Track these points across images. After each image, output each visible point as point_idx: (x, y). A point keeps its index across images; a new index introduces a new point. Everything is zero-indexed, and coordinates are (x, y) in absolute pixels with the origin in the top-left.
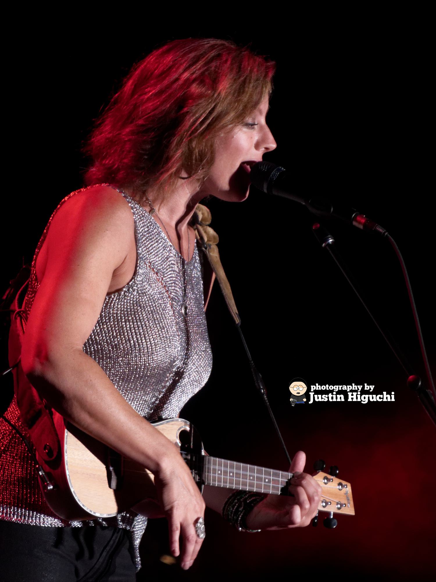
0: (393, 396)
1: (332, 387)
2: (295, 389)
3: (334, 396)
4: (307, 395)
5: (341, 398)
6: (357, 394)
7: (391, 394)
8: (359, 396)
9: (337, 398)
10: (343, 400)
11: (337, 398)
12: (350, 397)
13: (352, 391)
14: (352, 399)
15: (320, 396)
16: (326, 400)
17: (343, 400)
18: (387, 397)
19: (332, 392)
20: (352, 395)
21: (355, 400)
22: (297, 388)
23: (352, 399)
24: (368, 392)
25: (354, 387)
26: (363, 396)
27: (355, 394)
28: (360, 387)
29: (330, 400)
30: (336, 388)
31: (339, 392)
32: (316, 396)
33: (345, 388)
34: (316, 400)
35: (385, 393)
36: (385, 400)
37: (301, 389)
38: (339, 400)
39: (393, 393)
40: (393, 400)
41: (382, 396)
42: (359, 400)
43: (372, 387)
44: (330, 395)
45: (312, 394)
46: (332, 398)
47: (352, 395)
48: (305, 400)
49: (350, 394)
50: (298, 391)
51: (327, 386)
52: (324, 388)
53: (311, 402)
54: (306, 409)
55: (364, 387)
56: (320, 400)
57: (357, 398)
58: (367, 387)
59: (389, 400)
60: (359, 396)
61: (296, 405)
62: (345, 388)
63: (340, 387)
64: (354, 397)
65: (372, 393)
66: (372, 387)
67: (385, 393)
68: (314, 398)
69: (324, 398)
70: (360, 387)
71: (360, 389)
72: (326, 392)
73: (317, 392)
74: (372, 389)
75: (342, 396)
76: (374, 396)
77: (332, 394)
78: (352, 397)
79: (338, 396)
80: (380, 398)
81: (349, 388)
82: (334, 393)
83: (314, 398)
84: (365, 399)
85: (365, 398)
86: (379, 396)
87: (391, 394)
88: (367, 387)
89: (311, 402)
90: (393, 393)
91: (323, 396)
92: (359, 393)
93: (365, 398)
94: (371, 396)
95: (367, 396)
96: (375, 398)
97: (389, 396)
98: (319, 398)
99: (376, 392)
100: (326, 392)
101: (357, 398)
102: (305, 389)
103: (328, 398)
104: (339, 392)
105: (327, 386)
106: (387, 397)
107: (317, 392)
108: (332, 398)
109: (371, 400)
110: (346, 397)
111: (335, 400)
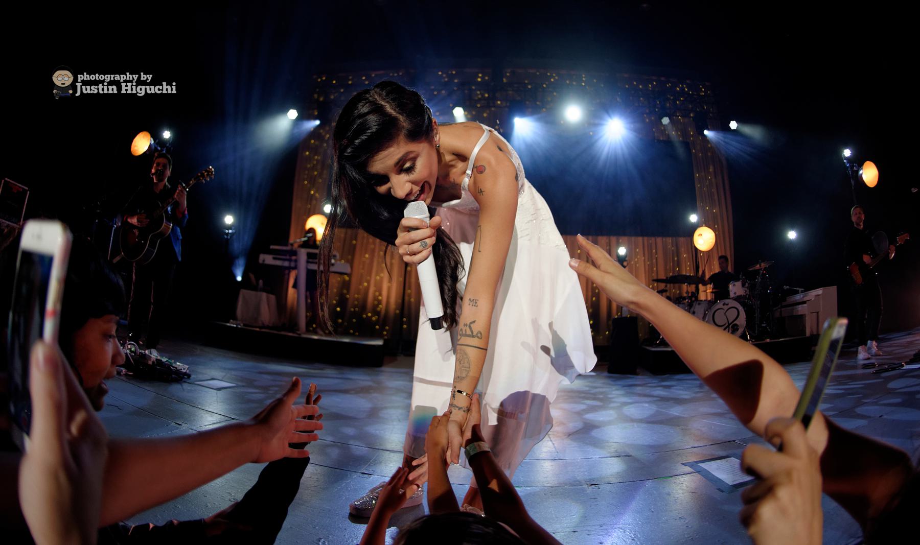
0: (174, 88)
1: (102, 77)
3: (105, 88)
4: (73, 86)
5: (113, 89)
6: (132, 85)
7: (171, 85)
8: (134, 87)
10: (115, 92)
12: (124, 88)
13: (126, 81)
15: (88, 87)
16: (96, 91)
17: (115, 92)
18: (168, 89)
19: (102, 82)
21: (129, 91)
22: (62, 78)
24: (144, 83)
25: (129, 76)
26: (139, 87)
27: (129, 84)
28: (136, 77)
29: (101, 92)
30: (108, 78)
31: (111, 83)
32: (84, 87)
33: (117, 77)
34: (84, 92)
35: (164, 84)
36: (165, 92)
38: (110, 92)
40: (174, 91)
42: (134, 92)
43: (150, 77)
44: (100, 86)
45: (79, 85)
46: (103, 89)
48: (71, 92)
49: (123, 85)
53: (78, 94)
54: (71, 102)
55: (140, 77)
56: (89, 91)
58: (143, 77)
59: (169, 92)
60: (134, 87)
61: (61, 98)
62: (117, 77)
64: (129, 88)
65: (150, 84)
66: (150, 77)
67: (164, 84)
69: (93, 90)
70: (136, 77)
72: (96, 83)
73: (85, 83)
75: (115, 87)
76: (152, 87)
77: (103, 85)
78: (126, 89)
79: (110, 87)
81: (122, 78)
84: (141, 91)
86: (157, 87)
87: (171, 85)
88: (143, 77)
89: (78, 94)
91: (93, 87)
94: (148, 87)
95: (143, 87)
96: (153, 90)
97: (169, 87)
98: (87, 90)
99: (154, 83)
100: (96, 83)
104: (111, 83)
106: (168, 89)
107: (85, 83)
108: (103, 89)
109: (149, 92)
111: (106, 92)
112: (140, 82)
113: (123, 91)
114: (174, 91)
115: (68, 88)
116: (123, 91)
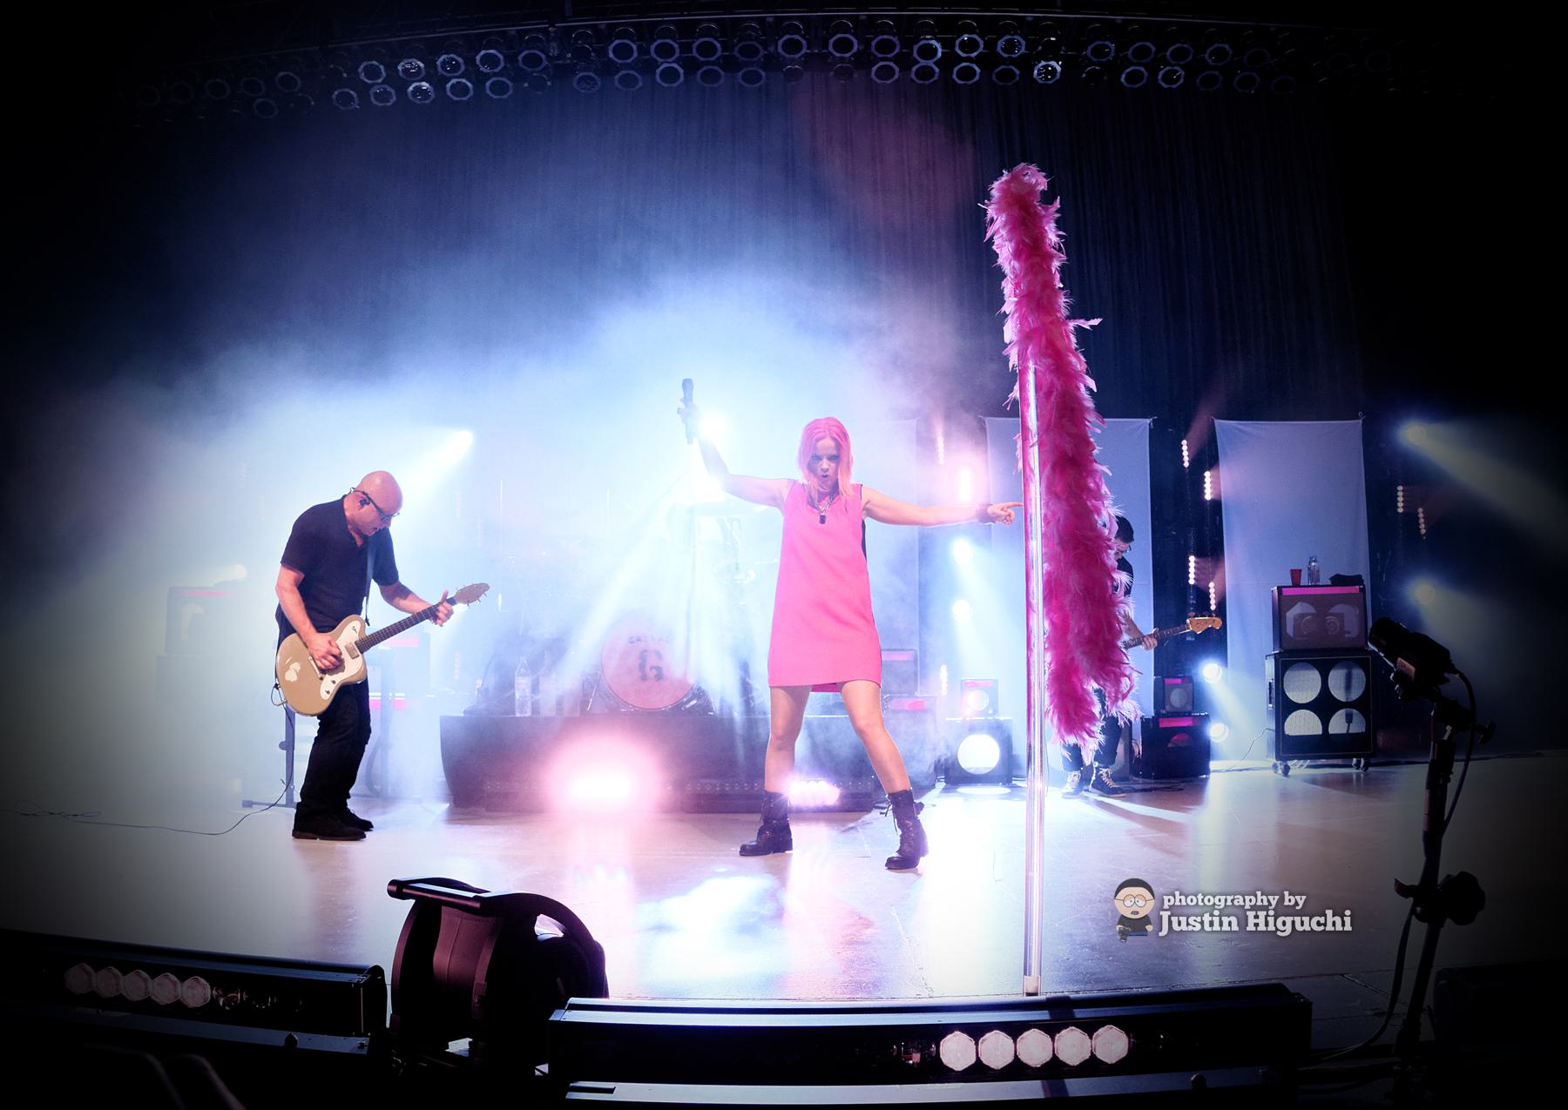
0: (1348, 920)
2: (1128, 903)
3: (1216, 920)
8: (1271, 920)
9: (1221, 924)
11: (1221, 924)
12: (1251, 921)
13: (1253, 908)
14: (1256, 925)
15: (1183, 919)
17: (1235, 927)
20: (1256, 917)
21: (1262, 928)
23: (1256, 925)
24: (1292, 911)
26: (1280, 920)
27: (1262, 914)
28: (1274, 900)
29: (1207, 928)
34: (1175, 927)
35: (1329, 913)
36: (1330, 928)
37: (1141, 903)
38: (1226, 927)
39: (1348, 912)
40: (1348, 928)
41: (1322, 920)
42: (1271, 928)
43: (1301, 900)
45: (1165, 915)
46: (1211, 924)
47: (1256, 917)
49: (1251, 914)
50: (1135, 908)
51: (1200, 897)
52: (1191, 901)
55: (1282, 899)
56: (1184, 927)
57: (1267, 924)
58: (1289, 900)
59: (1339, 928)
60: (1271, 920)
62: (1239, 901)
63: (1230, 898)
64: (1261, 921)
65: (1301, 914)
66: (1301, 900)
67: (1329, 913)
68: (1170, 922)
71: (1274, 903)
74: (1301, 903)
76: (1306, 919)
79: (1225, 920)
80: (1319, 924)
82: (1216, 913)
83: (1170, 922)
84: (1285, 926)
85: (1284, 923)
86: (1315, 919)
90: (1348, 912)
91: (1191, 920)
92: (1271, 913)
93: (1284, 923)
94: (1298, 919)
95: (1289, 920)
96: (1308, 924)
97: (1338, 920)
101: (1267, 924)
102: (1151, 904)
103: (1202, 923)
105: (1200, 897)
106: (1335, 923)
108: (1211, 924)
109: (1299, 927)
110: (1243, 922)
112: (1282, 910)
113: (1251, 927)
114: (1348, 928)
115: (1146, 920)
116: (1251, 927)
